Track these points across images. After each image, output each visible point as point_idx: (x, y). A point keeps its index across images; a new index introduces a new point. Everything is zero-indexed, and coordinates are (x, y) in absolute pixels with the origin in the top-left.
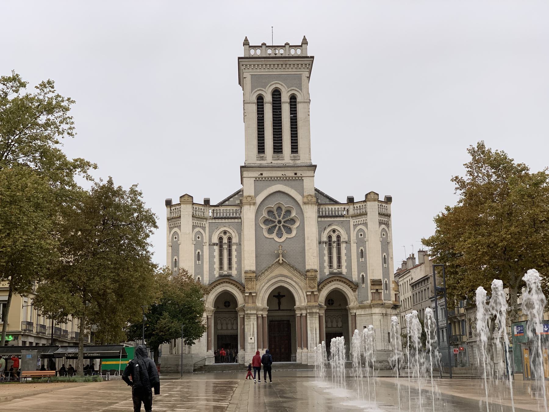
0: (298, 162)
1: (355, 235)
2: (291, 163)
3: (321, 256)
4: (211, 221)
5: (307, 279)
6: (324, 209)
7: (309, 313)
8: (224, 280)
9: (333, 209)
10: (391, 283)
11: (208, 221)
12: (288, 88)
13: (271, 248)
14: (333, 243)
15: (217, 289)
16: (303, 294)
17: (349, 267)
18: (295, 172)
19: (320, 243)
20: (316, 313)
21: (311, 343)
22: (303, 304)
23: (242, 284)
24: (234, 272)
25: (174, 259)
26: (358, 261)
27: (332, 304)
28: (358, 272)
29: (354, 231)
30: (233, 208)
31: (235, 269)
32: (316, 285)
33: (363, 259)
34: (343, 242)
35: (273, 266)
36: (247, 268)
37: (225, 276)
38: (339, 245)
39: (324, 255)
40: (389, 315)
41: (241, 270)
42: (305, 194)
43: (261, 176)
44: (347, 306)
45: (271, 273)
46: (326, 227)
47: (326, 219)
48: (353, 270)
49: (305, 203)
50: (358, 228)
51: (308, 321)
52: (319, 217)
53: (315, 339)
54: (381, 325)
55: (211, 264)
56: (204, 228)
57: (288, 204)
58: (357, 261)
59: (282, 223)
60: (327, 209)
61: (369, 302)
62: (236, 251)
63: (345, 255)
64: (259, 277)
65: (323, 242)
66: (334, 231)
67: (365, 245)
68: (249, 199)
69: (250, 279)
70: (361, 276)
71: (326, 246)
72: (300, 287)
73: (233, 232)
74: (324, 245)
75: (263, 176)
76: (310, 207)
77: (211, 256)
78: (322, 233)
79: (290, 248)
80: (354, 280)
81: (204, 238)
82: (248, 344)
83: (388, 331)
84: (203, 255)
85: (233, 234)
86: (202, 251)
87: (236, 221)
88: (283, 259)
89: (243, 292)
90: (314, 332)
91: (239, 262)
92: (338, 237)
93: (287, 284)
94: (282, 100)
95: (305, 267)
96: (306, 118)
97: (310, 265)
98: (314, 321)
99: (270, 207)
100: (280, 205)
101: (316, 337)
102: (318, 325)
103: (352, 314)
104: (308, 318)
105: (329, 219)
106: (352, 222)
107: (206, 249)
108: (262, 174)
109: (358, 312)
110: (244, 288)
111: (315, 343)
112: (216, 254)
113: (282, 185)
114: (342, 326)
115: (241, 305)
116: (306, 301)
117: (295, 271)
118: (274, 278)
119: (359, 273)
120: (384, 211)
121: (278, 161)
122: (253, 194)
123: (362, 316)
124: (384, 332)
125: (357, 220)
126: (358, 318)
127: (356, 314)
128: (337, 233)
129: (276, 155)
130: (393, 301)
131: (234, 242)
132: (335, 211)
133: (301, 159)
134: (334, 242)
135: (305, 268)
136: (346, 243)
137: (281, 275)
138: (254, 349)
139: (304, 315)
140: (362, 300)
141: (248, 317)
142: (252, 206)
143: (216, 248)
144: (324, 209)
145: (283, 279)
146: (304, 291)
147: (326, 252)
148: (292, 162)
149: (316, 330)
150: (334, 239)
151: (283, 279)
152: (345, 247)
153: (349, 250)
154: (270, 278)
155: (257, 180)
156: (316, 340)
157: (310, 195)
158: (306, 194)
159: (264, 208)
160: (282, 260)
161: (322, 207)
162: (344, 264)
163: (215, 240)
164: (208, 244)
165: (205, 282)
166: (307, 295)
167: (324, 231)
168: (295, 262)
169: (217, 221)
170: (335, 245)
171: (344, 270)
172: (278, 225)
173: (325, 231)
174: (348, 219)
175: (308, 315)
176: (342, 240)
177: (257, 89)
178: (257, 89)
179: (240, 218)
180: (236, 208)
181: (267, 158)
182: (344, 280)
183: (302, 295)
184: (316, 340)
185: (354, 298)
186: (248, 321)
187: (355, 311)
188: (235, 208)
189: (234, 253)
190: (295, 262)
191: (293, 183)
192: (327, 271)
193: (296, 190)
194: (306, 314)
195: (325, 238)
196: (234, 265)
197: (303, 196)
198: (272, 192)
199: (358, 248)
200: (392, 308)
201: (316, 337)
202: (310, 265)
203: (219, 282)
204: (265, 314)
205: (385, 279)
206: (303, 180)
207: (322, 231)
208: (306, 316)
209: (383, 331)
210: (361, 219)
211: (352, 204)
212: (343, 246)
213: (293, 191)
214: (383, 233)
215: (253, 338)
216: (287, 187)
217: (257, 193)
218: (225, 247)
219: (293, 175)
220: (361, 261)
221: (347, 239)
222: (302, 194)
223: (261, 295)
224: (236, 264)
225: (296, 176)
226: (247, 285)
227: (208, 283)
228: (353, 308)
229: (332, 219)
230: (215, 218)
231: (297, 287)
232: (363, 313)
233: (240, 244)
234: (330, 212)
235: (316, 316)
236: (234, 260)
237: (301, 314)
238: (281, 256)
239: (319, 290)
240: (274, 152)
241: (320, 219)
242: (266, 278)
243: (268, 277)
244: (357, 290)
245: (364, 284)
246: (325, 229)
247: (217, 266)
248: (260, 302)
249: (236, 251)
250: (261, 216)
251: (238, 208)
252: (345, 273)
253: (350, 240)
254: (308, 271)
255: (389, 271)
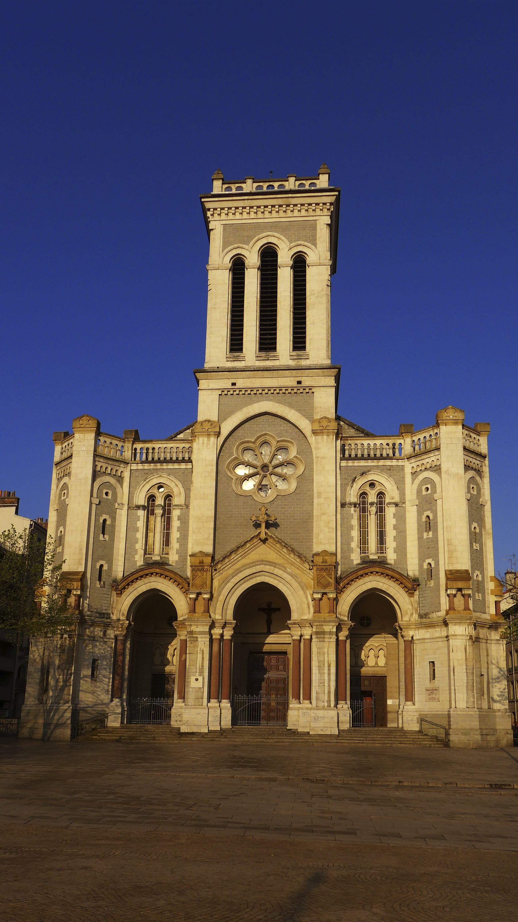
0: (304, 363)
1: (415, 492)
2: (292, 363)
3: (346, 528)
4: (134, 467)
5: (315, 568)
6: (353, 446)
7: (317, 633)
8: (152, 570)
9: (372, 445)
10: (488, 580)
11: (129, 468)
12: (290, 243)
13: (247, 514)
14: (369, 506)
15: (136, 587)
16: (307, 598)
17: (401, 550)
18: (299, 379)
19: (343, 505)
20: (330, 633)
21: (319, 691)
22: (306, 617)
23: (186, 579)
24: (173, 558)
25: (59, 531)
26: (420, 538)
27: (369, 625)
28: (420, 559)
29: (413, 483)
30: (178, 445)
31: (175, 551)
32: (332, 581)
33: (431, 533)
34: (389, 503)
35: (248, 545)
36: (197, 549)
37: (156, 564)
38: (381, 510)
39: (352, 527)
40: (484, 641)
41: (187, 553)
42: (317, 417)
43: (233, 387)
44: (396, 624)
45: (243, 557)
46: (355, 478)
47: (357, 463)
48: (409, 556)
49: (315, 432)
50: (421, 477)
51: (314, 649)
52: (343, 458)
53: (326, 684)
54: (466, 659)
55: (130, 542)
56: (120, 479)
57: (283, 436)
58: (419, 538)
59: (271, 469)
60: (359, 446)
61: (442, 613)
62: (178, 520)
63: (394, 529)
64: (219, 566)
65: (350, 504)
66: (372, 485)
67: (434, 508)
68: (207, 426)
69: (201, 568)
70: (425, 566)
71: (355, 511)
72: (299, 583)
73: (175, 486)
74: (352, 509)
75: (235, 387)
76: (325, 440)
77: (131, 529)
78: (349, 488)
79: (284, 513)
80: (411, 573)
81: (119, 495)
82: (191, 689)
83: (481, 672)
84: (113, 526)
85: (175, 490)
86: (114, 519)
87: (183, 466)
88: (267, 531)
89: (186, 592)
90: (326, 671)
91: (184, 539)
92: (381, 495)
93: (275, 579)
94: (279, 263)
95: (312, 548)
96: (322, 290)
97: (321, 543)
98: (326, 650)
99: (248, 442)
100: (268, 438)
101: (329, 680)
102: (333, 657)
103: (405, 639)
104: (313, 644)
105: (363, 463)
106: (408, 466)
107: (122, 515)
108: (234, 384)
109: (419, 634)
110: (189, 584)
111: (326, 692)
112: (141, 524)
113: (271, 403)
114: (386, 664)
115: (182, 616)
116: (312, 610)
117: (292, 555)
118: (248, 568)
119: (421, 560)
120: (472, 447)
121: (267, 361)
122: (215, 418)
123: (426, 641)
124: (473, 673)
125: (418, 463)
126: (417, 648)
127: (414, 638)
128: (378, 488)
129: (263, 354)
130: (491, 615)
131: (176, 504)
132: (375, 449)
133: (310, 357)
134: (372, 504)
135: (312, 551)
136: (396, 505)
137: (262, 561)
138: (200, 700)
139: (308, 637)
140: (426, 611)
141: (192, 639)
142: (213, 439)
143: (141, 513)
144: (353, 445)
145: (267, 568)
146: (308, 592)
147: (355, 522)
148: (293, 364)
149: (329, 666)
150: (372, 497)
151: (267, 568)
152: (394, 514)
153: (401, 518)
154: (241, 567)
155: (223, 393)
156: (329, 686)
157: (326, 418)
158: (318, 417)
159: (235, 444)
160: (266, 533)
161: (349, 442)
162: (390, 543)
163: (141, 499)
164: (126, 507)
165: (114, 574)
166: (314, 599)
167: (353, 483)
168: (293, 539)
169: (146, 468)
170: (373, 509)
171: (391, 556)
172: (263, 473)
173: (355, 484)
174: (400, 463)
175: (314, 637)
176: (387, 500)
177: (232, 247)
178: (232, 247)
179: (190, 461)
180: (183, 445)
181: (246, 359)
182: (390, 573)
183: (305, 600)
184: (329, 686)
185: (410, 607)
186: (192, 645)
187: (411, 633)
188: (181, 446)
189: (175, 524)
190: (293, 539)
191: (295, 398)
192: (356, 558)
193: (299, 411)
194: (311, 636)
195: (353, 496)
196: (175, 544)
197: (313, 421)
198: (252, 413)
199: (420, 514)
200: (488, 628)
201: (329, 680)
202: (321, 543)
203: (141, 573)
204: (228, 634)
205: (476, 571)
206: (313, 393)
207: (347, 485)
208: (311, 639)
209: (471, 671)
210: (427, 460)
211: (410, 436)
212: (390, 512)
213: (293, 411)
214: (472, 486)
215: (200, 679)
216: (281, 405)
217: (223, 416)
218: (159, 512)
219: (295, 384)
220: (425, 537)
221: (397, 499)
222: (309, 416)
223: (222, 598)
224: (177, 542)
225: (299, 385)
226: (193, 579)
227: (120, 575)
228: (409, 626)
229: (370, 463)
230: (142, 463)
231: (295, 584)
232: (427, 636)
233: (187, 506)
234: (366, 451)
235: (331, 640)
236: (175, 535)
237: (301, 636)
238: (263, 525)
239: (340, 591)
240: (261, 349)
241: (344, 463)
242: (233, 567)
243: (237, 566)
244: (417, 593)
245: (432, 582)
246: (354, 480)
247: (140, 546)
248: (219, 610)
249: (178, 520)
250: (230, 456)
251: (187, 446)
252: (392, 562)
253: (404, 499)
254: (317, 554)
255: (483, 558)
